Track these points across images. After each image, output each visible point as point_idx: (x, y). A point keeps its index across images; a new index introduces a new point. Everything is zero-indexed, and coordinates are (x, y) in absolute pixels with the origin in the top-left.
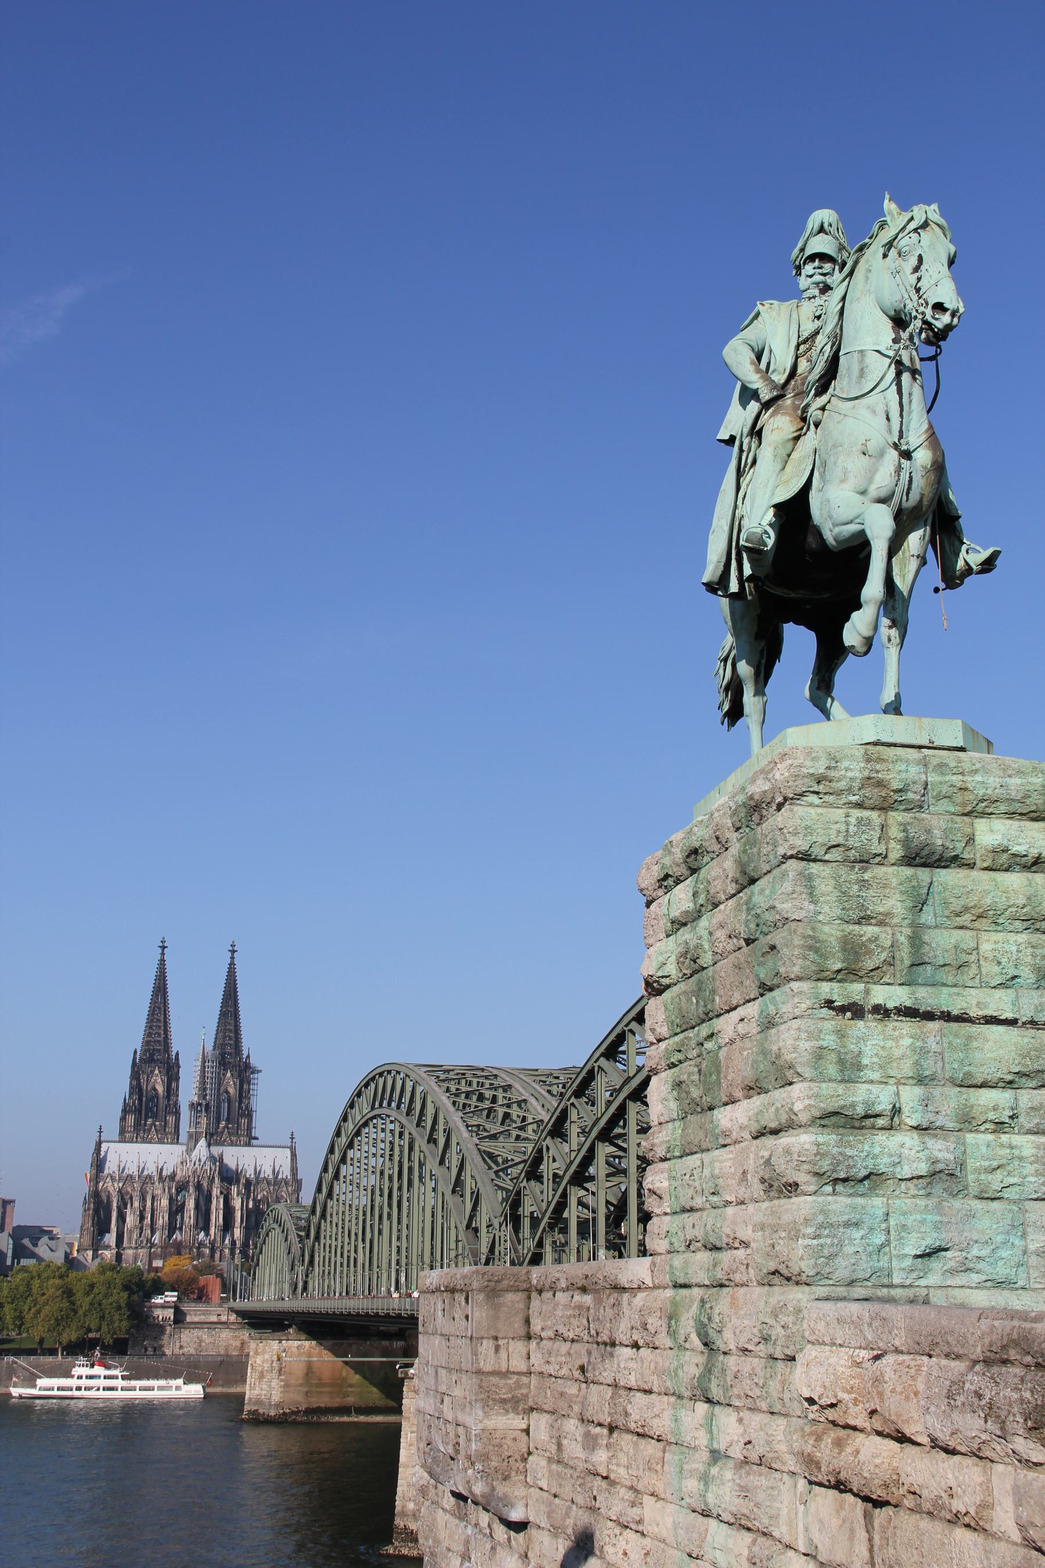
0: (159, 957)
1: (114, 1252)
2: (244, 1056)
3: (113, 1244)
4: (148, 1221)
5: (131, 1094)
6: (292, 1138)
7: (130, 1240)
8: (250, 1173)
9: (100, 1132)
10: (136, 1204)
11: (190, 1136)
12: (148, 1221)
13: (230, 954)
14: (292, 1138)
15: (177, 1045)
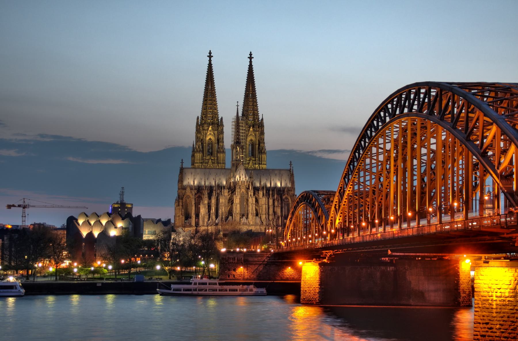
0: (208, 63)
1: (195, 228)
2: (260, 119)
3: (193, 223)
4: (213, 210)
5: (197, 142)
6: (291, 165)
7: (203, 221)
8: (268, 185)
9: (182, 163)
10: (206, 202)
11: (233, 165)
12: (213, 210)
13: (249, 60)
14: (291, 165)
15: (221, 114)
